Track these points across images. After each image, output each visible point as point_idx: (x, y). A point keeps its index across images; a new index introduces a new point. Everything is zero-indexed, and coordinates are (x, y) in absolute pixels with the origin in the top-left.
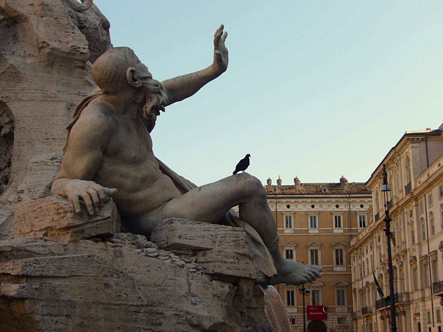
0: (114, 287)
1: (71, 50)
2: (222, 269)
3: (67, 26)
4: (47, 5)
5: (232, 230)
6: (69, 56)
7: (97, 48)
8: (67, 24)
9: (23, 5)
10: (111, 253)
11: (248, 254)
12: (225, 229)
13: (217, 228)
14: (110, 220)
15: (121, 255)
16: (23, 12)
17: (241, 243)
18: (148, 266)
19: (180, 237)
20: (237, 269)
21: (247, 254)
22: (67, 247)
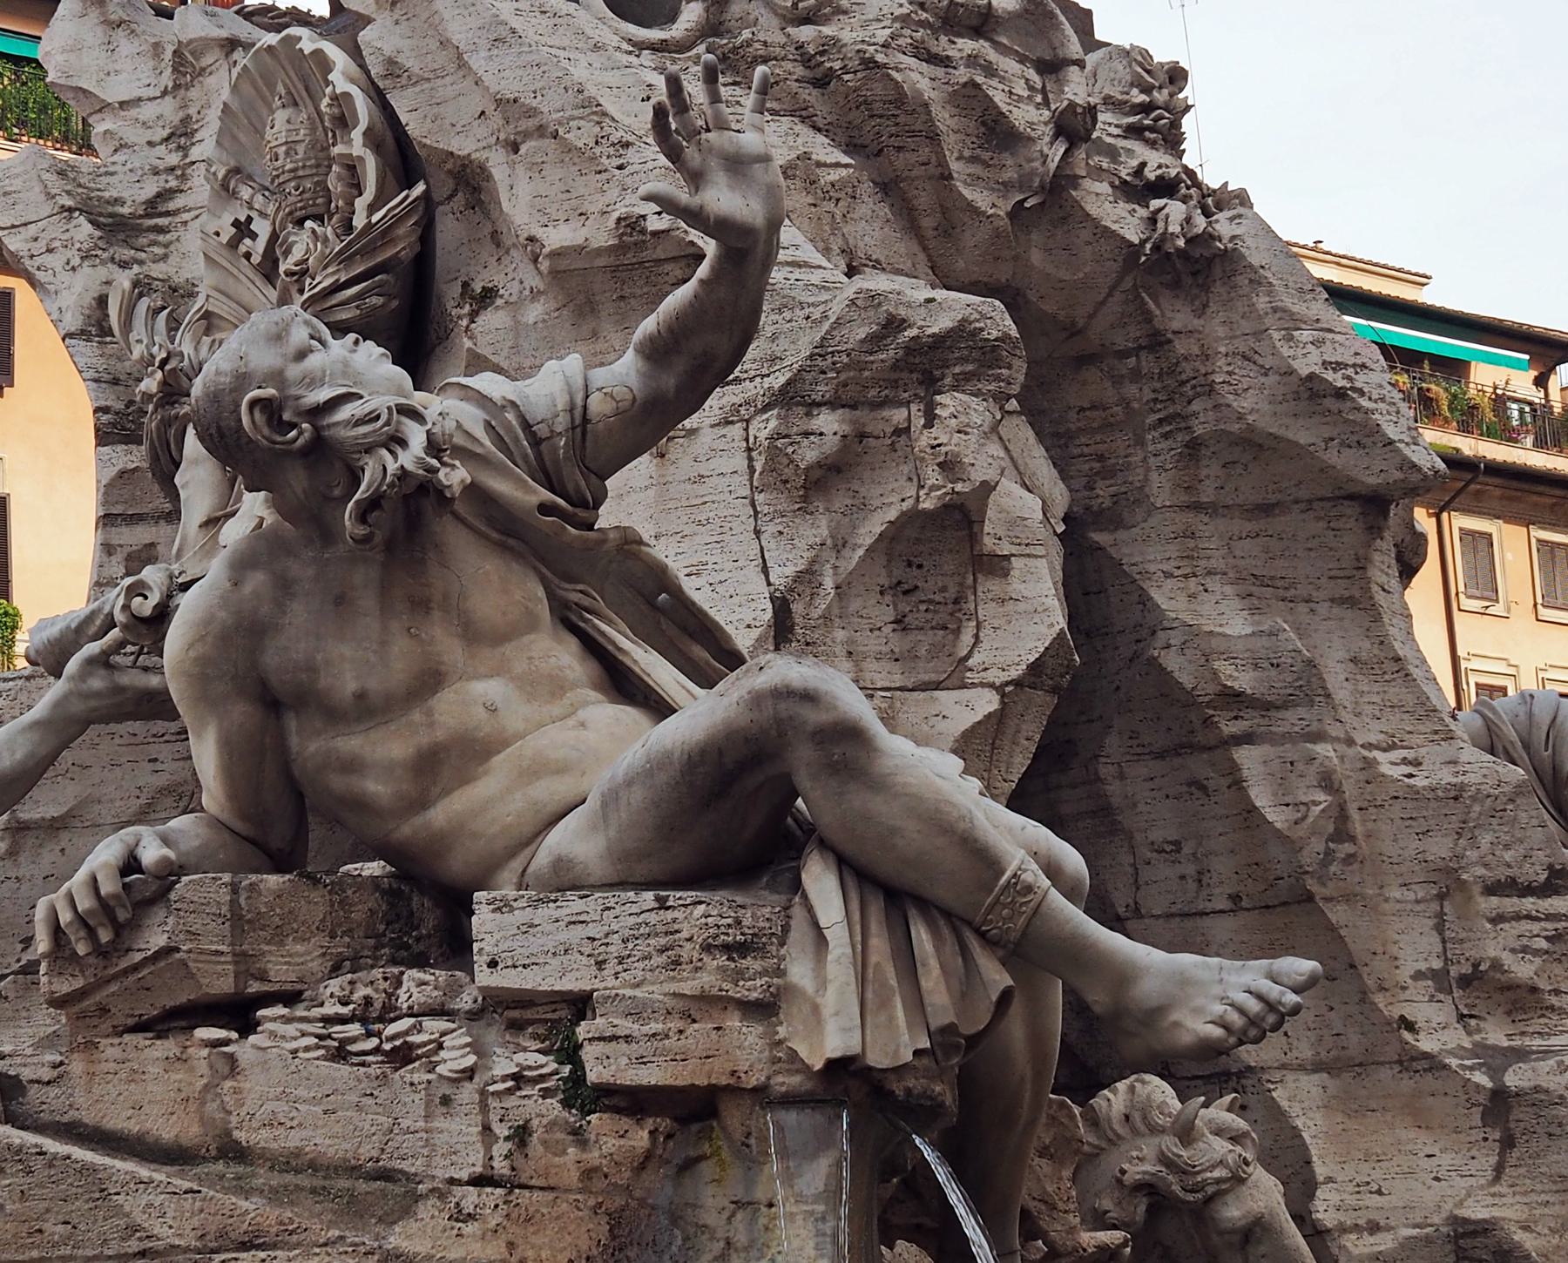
0: (9, 1208)
1: (622, 234)
2: (613, 1068)
3: (598, 150)
4: (515, 101)
5: (652, 909)
6: (630, 258)
7: (913, 133)
8: (597, 143)
9: (462, 123)
10: (203, 1067)
11: (721, 990)
12: (635, 909)
13: (608, 909)
14: (177, 956)
15: (232, 1070)
16: (465, 152)
17: (685, 957)
18: (328, 1096)
19: (493, 964)
20: (678, 1057)
21: (715, 991)
22: (62, 1068)
